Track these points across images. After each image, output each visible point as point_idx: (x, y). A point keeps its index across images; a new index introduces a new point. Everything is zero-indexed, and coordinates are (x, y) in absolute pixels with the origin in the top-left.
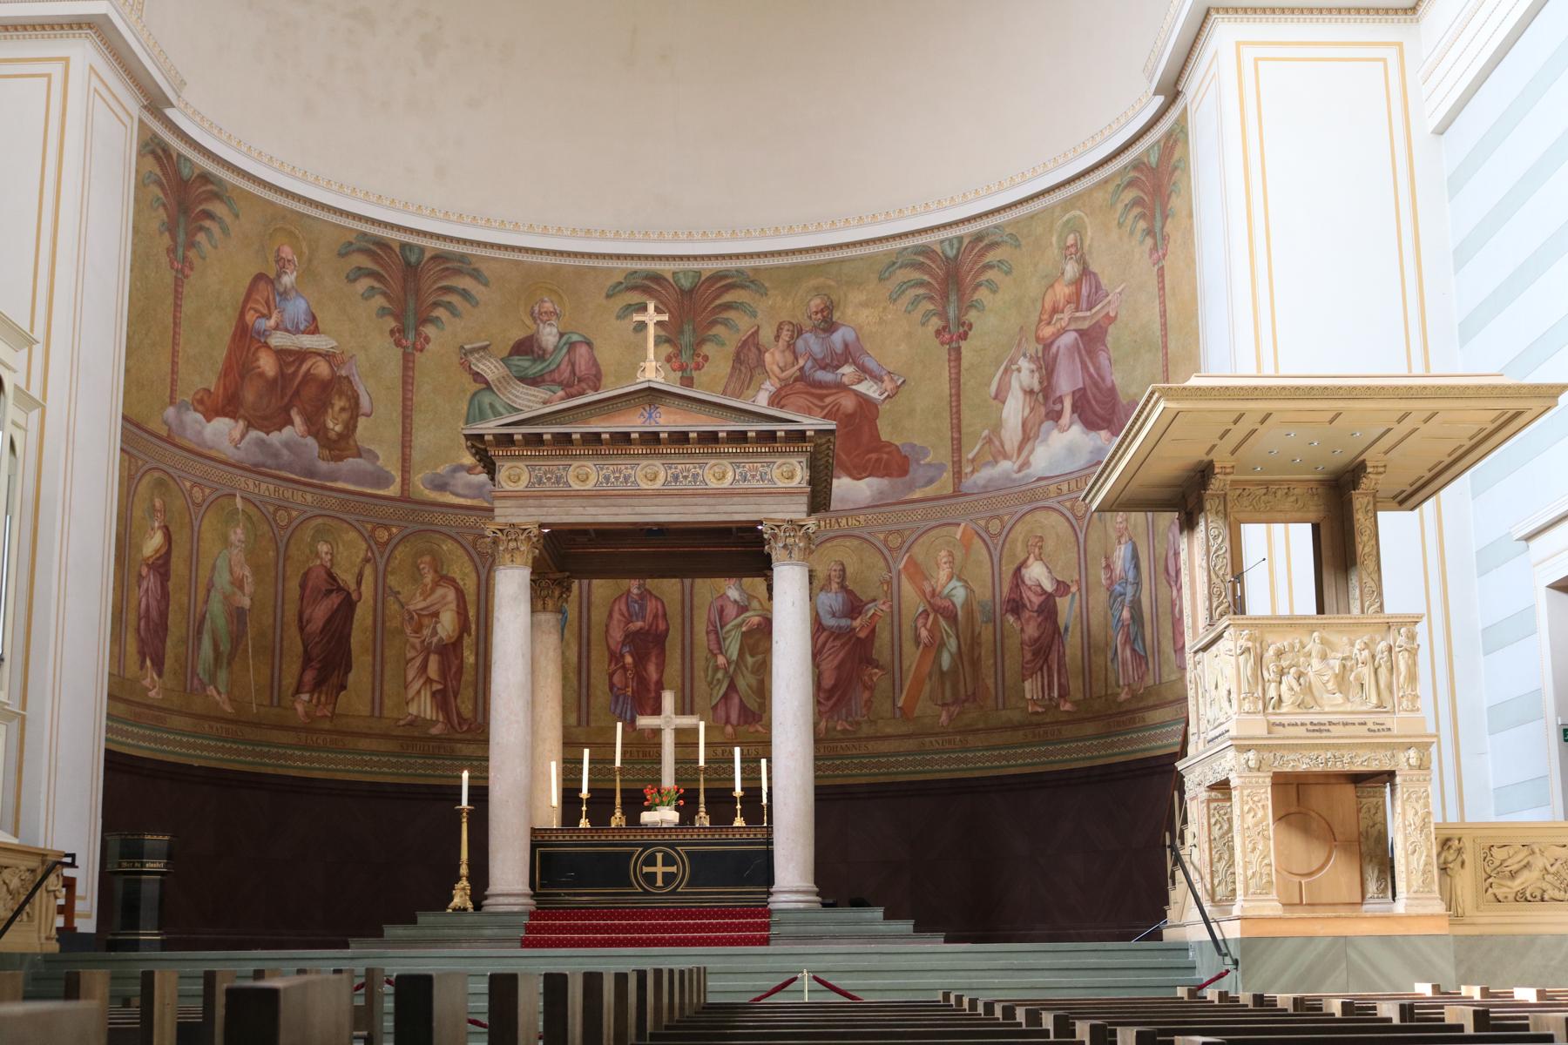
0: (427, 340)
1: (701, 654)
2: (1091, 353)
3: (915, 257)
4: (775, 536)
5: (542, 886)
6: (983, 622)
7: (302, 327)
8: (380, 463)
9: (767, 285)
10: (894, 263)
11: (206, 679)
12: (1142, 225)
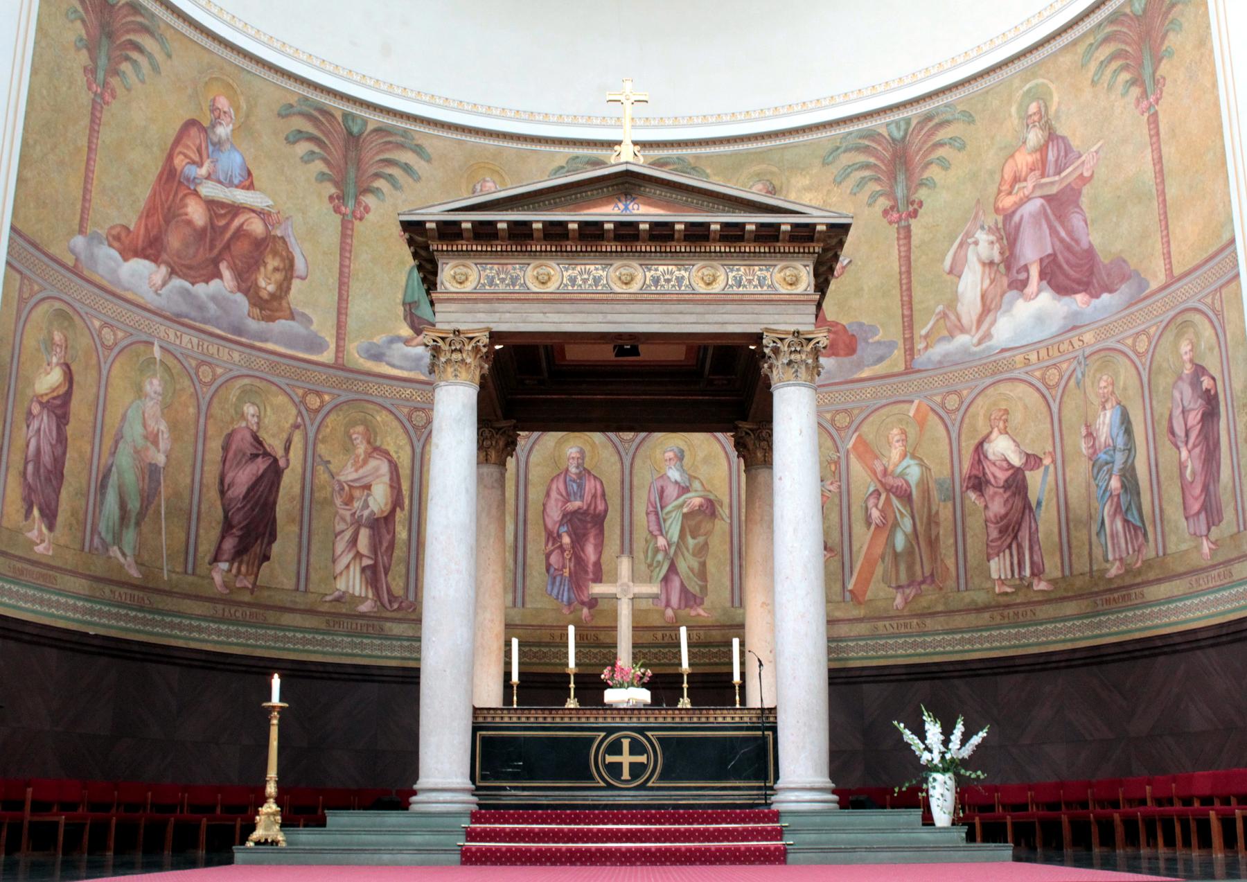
0: (367, 209)
1: (640, 535)
2: (1061, 218)
3: (860, 141)
4: (776, 351)
5: (484, 778)
6: (940, 500)
7: (236, 181)
8: (314, 327)
9: (708, 171)
10: (838, 148)
11: (109, 538)
12: (1125, 76)
